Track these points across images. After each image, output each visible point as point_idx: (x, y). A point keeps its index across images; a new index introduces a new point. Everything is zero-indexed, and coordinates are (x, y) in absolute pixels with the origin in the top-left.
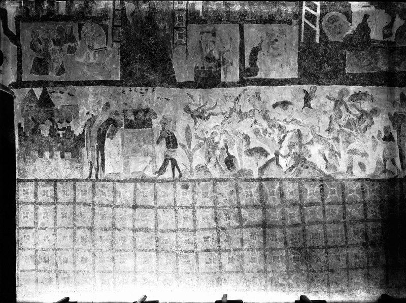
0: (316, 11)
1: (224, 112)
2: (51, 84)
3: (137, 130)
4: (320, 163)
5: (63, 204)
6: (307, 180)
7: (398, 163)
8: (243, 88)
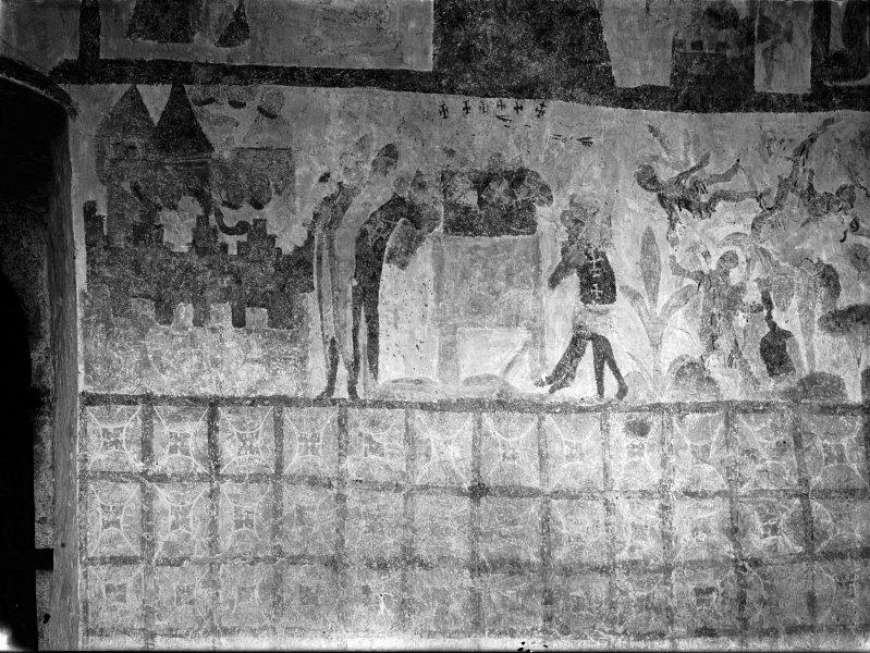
1: (760, 189)
2: (201, 73)
3: (485, 241)
5: (238, 479)
8: (820, 116)
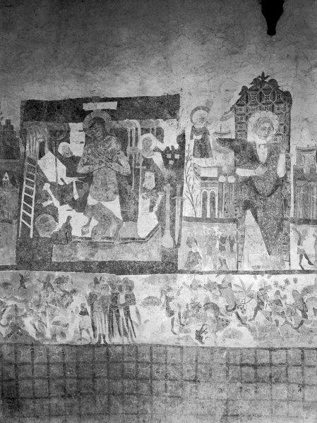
0: (30, 213)
4: (31, 331)
6: (21, 345)
7: (92, 333)
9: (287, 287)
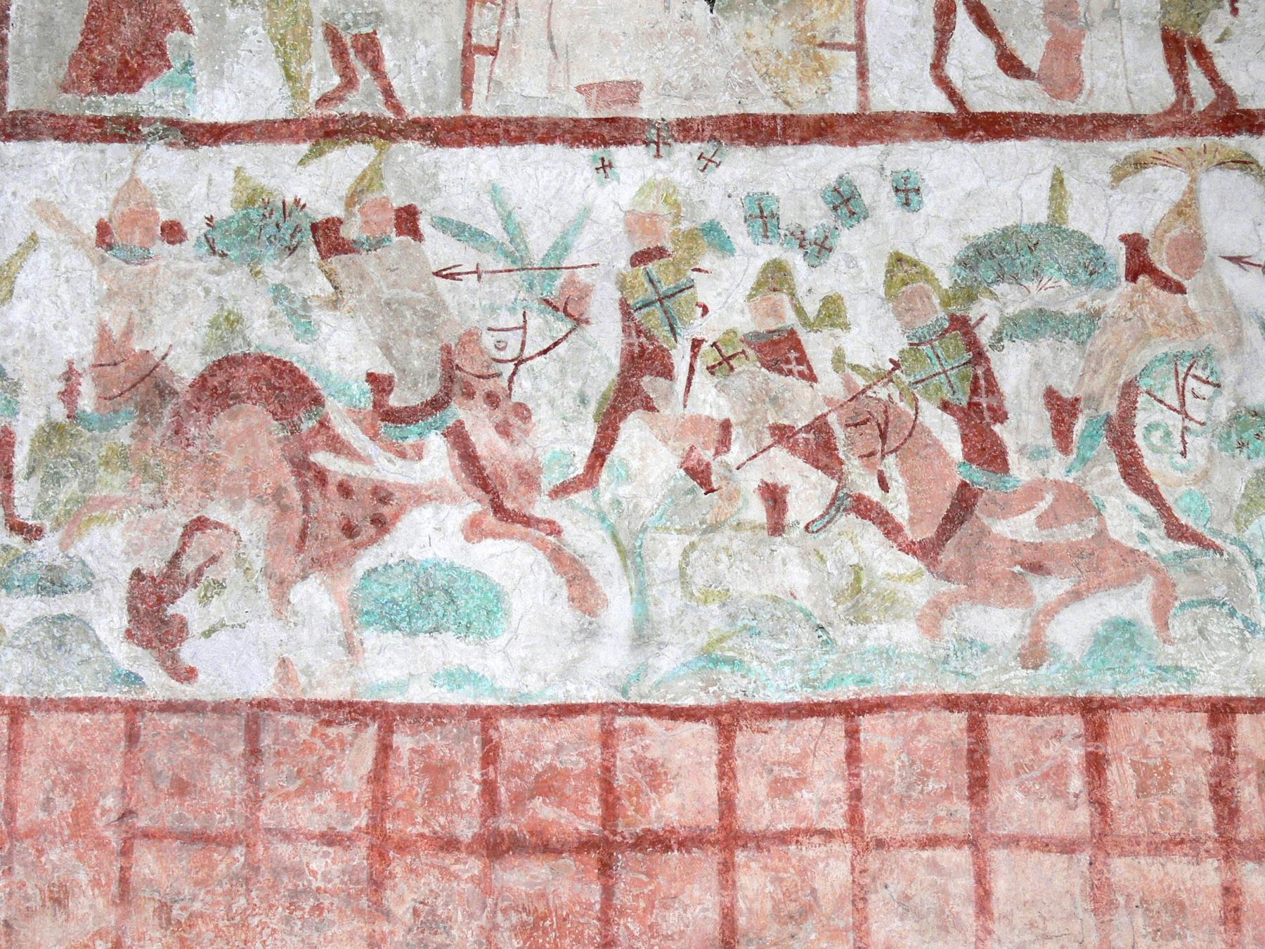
9: (850, 240)
